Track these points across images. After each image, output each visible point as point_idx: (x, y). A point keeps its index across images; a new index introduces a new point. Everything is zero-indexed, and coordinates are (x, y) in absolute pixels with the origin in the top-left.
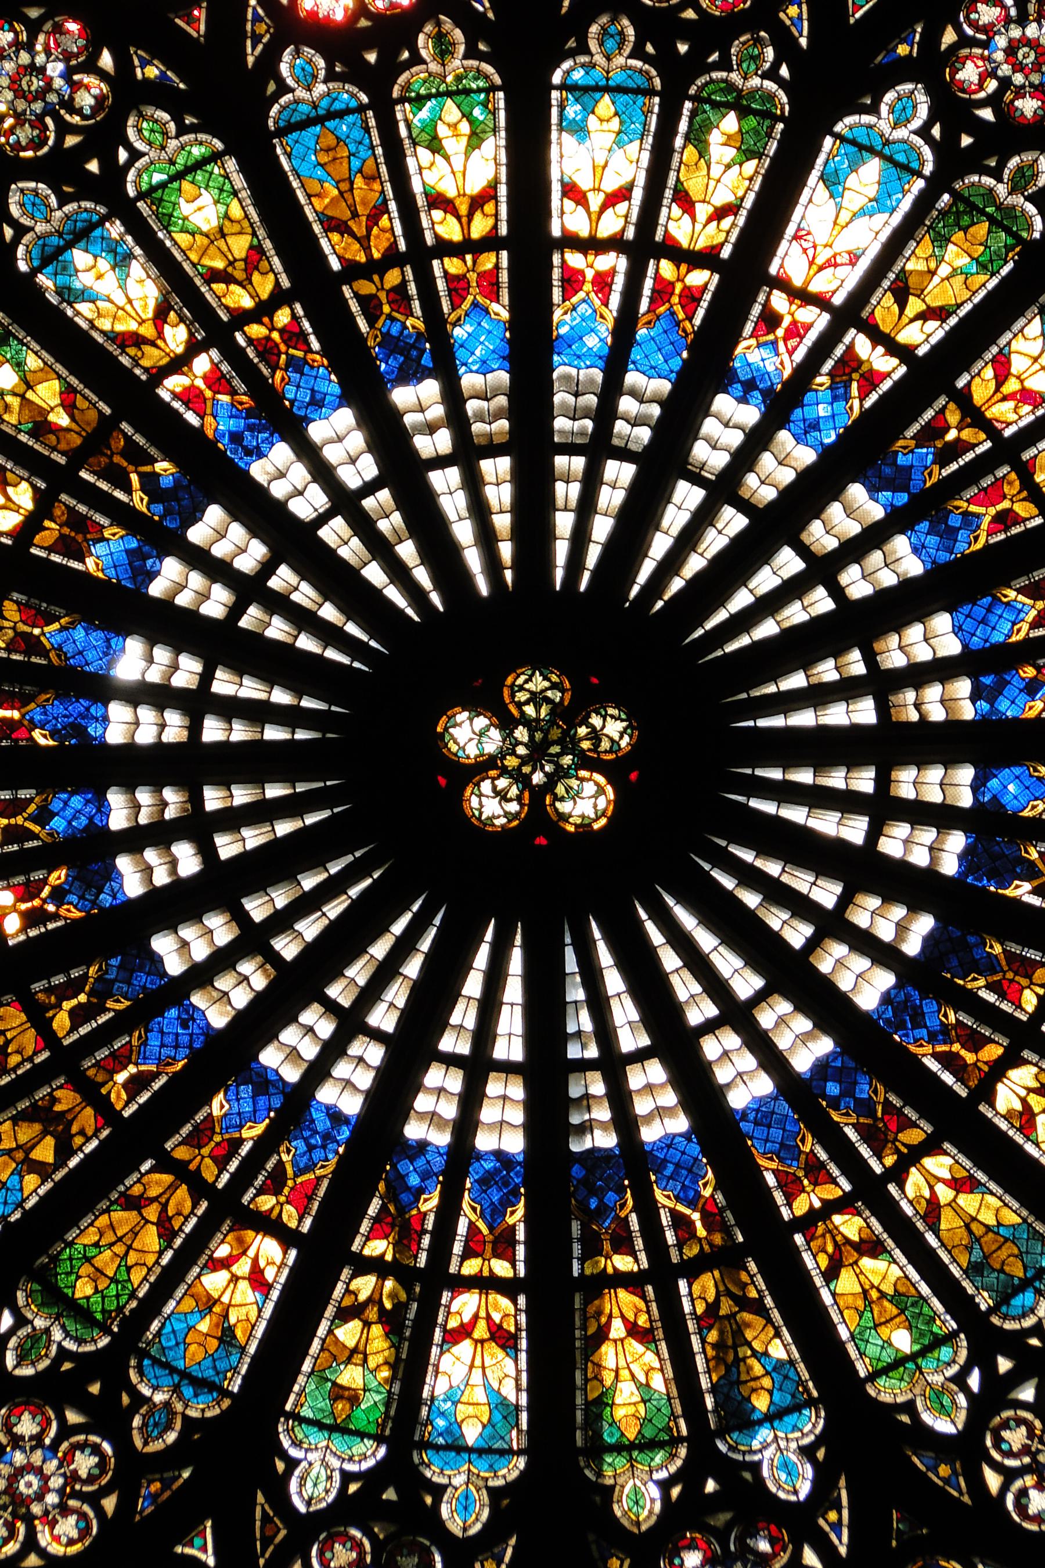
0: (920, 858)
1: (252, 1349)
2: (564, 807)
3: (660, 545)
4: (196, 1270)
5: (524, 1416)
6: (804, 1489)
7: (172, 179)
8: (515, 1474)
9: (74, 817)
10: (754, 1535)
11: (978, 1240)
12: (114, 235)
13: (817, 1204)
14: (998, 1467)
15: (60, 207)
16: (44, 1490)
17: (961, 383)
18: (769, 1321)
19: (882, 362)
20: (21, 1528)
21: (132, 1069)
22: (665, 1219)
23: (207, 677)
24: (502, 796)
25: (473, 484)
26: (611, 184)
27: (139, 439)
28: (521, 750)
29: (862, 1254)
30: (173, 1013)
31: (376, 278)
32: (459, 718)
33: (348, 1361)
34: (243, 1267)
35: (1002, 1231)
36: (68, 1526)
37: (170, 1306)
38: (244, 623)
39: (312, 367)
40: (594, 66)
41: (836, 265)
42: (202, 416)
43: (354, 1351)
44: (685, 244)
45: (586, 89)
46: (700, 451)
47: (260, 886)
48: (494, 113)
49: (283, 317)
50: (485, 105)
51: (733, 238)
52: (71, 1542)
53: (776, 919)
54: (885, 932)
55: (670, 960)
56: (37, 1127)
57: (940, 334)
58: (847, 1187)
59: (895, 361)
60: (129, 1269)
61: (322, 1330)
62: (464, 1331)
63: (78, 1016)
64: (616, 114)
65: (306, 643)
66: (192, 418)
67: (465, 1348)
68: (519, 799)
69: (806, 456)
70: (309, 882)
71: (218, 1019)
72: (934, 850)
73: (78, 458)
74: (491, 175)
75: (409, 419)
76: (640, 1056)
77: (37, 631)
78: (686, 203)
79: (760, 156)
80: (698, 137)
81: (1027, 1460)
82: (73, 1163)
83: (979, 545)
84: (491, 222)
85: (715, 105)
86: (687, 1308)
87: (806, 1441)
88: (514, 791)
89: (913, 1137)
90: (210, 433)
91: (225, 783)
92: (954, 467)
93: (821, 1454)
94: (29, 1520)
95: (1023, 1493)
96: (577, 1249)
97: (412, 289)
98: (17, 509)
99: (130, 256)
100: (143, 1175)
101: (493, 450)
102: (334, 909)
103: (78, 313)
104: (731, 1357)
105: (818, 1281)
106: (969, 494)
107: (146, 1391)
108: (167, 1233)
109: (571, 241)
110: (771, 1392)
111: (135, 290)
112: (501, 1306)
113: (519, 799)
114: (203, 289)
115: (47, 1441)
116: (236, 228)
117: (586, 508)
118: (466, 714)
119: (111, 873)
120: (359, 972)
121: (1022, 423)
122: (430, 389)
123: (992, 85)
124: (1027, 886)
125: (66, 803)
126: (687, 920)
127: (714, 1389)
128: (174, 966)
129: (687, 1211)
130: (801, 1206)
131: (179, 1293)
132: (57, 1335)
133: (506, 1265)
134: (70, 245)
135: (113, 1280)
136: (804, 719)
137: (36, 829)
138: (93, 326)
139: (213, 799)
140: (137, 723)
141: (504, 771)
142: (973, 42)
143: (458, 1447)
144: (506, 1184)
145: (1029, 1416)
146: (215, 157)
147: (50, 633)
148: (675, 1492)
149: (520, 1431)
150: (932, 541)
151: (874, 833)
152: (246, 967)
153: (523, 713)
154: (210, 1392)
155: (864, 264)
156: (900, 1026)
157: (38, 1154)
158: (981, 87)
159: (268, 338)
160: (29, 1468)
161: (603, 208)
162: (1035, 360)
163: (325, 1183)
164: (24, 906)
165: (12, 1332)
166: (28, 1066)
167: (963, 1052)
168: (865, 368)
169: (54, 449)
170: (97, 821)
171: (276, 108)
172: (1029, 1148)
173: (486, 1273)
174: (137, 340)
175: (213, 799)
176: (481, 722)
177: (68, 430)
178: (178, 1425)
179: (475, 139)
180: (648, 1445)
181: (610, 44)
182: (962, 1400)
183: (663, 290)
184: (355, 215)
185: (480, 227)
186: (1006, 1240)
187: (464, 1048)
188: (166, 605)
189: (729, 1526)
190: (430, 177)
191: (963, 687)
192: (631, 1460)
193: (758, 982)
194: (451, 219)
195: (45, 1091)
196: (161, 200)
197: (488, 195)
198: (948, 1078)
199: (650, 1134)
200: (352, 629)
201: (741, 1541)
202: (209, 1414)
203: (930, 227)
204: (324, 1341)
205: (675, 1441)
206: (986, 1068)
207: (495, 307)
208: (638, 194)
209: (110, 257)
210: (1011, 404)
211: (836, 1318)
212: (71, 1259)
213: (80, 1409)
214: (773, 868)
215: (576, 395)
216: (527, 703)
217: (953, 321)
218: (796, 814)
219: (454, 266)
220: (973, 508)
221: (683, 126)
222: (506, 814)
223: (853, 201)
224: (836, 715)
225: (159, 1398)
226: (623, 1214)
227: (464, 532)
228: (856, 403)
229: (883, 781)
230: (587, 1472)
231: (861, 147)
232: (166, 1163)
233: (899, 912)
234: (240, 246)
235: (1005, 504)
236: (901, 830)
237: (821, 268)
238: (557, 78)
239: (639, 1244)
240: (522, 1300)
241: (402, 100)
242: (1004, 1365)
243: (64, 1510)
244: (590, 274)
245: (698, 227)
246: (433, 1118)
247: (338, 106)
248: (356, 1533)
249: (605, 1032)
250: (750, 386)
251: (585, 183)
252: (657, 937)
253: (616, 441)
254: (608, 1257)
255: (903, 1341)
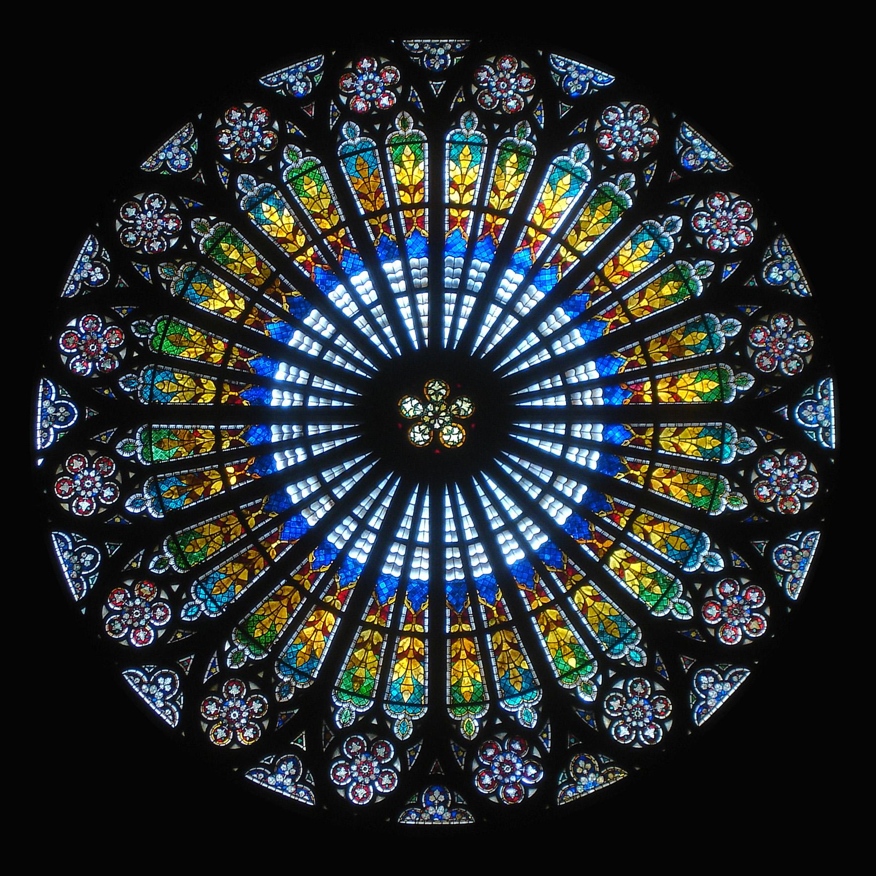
0: (582, 462)
1: (322, 660)
2: (446, 438)
3: (484, 331)
4: (301, 626)
5: (427, 690)
6: (534, 724)
7: (300, 175)
8: (422, 715)
9: (258, 437)
10: (514, 743)
11: (602, 621)
12: (278, 198)
13: (541, 605)
14: (609, 717)
15: (257, 186)
16: (241, 717)
17: (600, 267)
18: (522, 653)
19: (571, 259)
20: (232, 734)
21: (279, 542)
22: (482, 609)
23: (310, 380)
24: (422, 432)
25: (413, 303)
26: (468, 182)
27: (287, 282)
28: (430, 414)
29: (558, 626)
30: (294, 519)
31: (378, 218)
32: (407, 400)
33: (359, 667)
34: (320, 626)
35: (611, 618)
36: (249, 733)
37: (290, 642)
38: (325, 358)
39: (353, 254)
40: (462, 134)
41: (554, 218)
42: (310, 273)
43: (362, 661)
44: (496, 208)
45: (459, 143)
46: (500, 292)
47: (328, 467)
48: (423, 151)
49: (342, 233)
50: (420, 147)
51: (514, 205)
52: (251, 739)
53: (526, 486)
54: (568, 492)
55: (486, 503)
56: (241, 565)
57: (593, 247)
58: (552, 598)
59: (575, 258)
60: (275, 625)
61: (349, 653)
62: (404, 655)
63: (258, 519)
64: (470, 153)
65: (349, 367)
66: (306, 273)
67: (404, 661)
68: (429, 434)
69: (540, 296)
70: (348, 466)
71: (312, 522)
72: (587, 459)
73: (262, 289)
74: (422, 177)
75: (389, 276)
76: (474, 541)
77: (245, 360)
78: (496, 190)
79: (525, 172)
80: (501, 164)
81: (620, 714)
82: (254, 581)
83: (607, 333)
84: (422, 196)
85: (509, 151)
86: (490, 647)
87: (534, 704)
88: (427, 431)
89: (577, 578)
90: (314, 280)
91: (316, 424)
92: (597, 301)
93: (540, 709)
94: (235, 730)
95: (617, 728)
96: (448, 621)
97: (392, 223)
98: (239, 309)
99: (283, 206)
100: (282, 586)
101: (421, 290)
102: (357, 478)
103: (263, 229)
104: (506, 668)
105: (541, 637)
106: (603, 312)
107: (281, 677)
108: (290, 611)
109: (452, 205)
110: (522, 683)
111: (285, 220)
112: (420, 645)
113: (429, 434)
114: (312, 221)
115: (242, 697)
116: (325, 196)
117: (456, 314)
118: (409, 398)
119: (272, 462)
120: (366, 504)
121: (623, 284)
122: (397, 264)
123: (614, 145)
124: (623, 475)
125: (255, 431)
126: (492, 485)
127: (500, 681)
128: (295, 500)
129: (491, 607)
130: (534, 606)
131: (294, 636)
132: (247, 653)
133: (421, 627)
134: (261, 201)
135: (270, 630)
136: (538, 403)
137: (243, 441)
138: (269, 235)
139: (311, 430)
140: (283, 399)
141: (424, 423)
142: (606, 128)
143: (401, 703)
144: (422, 593)
145: (621, 695)
146: (317, 167)
147: (250, 361)
148: (484, 724)
149: (425, 697)
150: (588, 332)
151: (565, 451)
152: (323, 501)
153: (431, 399)
154: (306, 678)
155: (564, 217)
156: (573, 532)
157: (239, 577)
158: (609, 147)
159: (336, 241)
160: (235, 708)
161: (465, 192)
162: (629, 258)
163: (352, 591)
164: (238, 474)
165: (230, 650)
166: (238, 540)
167: (597, 543)
168: (564, 260)
169: (253, 285)
170: (267, 439)
171: (341, 147)
172: (622, 584)
173: (413, 630)
174: (284, 241)
175: (311, 430)
176: (415, 402)
177: (258, 277)
178: (293, 692)
179: (416, 163)
180: (473, 704)
181: (469, 124)
182: (595, 688)
183: (487, 226)
184: (370, 192)
185: (417, 198)
186: (613, 622)
187: (406, 537)
188: (295, 350)
189: (505, 738)
190: (399, 177)
191: (599, 392)
192: (467, 710)
193: (520, 512)
194: (407, 194)
195: (245, 550)
196: (296, 183)
197: (420, 186)
198: (591, 554)
199: (477, 574)
200: (367, 362)
201: (509, 745)
202: (305, 687)
203: (589, 203)
204: (350, 657)
205: (485, 702)
206: (606, 550)
207: (423, 231)
208: (478, 186)
209: (276, 206)
210: (619, 276)
211: (547, 653)
212: (253, 621)
213: (256, 683)
214: (526, 465)
215: (454, 268)
216: (433, 394)
217: (597, 241)
218: (535, 443)
219: (408, 214)
220: (604, 319)
221: (496, 159)
222: (424, 440)
223: (560, 192)
224: (551, 402)
225: (286, 680)
226: (466, 607)
227: (409, 323)
228: (560, 274)
229: (568, 430)
230: (450, 715)
231: (564, 170)
232: (291, 582)
233: (574, 484)
234: (326, 203)
235: (616, 318)
236: (575, 450)
237: (548, 219)
238: (448, 138)
239: (472, 619)
240: (427, 642)
241: (389, 145)
242: (612, 674)
243: (248, 726)
244: (459, 219)
245: (501, 201)
246: (393, 565)
247: (364, 147)
248: (362, 739)
249: (460, 531)
250: (519, 268)
251: (458, 181)
252: (481, 493)
253: (468, 288)
254: (460, 625)
255: (572, 662)
